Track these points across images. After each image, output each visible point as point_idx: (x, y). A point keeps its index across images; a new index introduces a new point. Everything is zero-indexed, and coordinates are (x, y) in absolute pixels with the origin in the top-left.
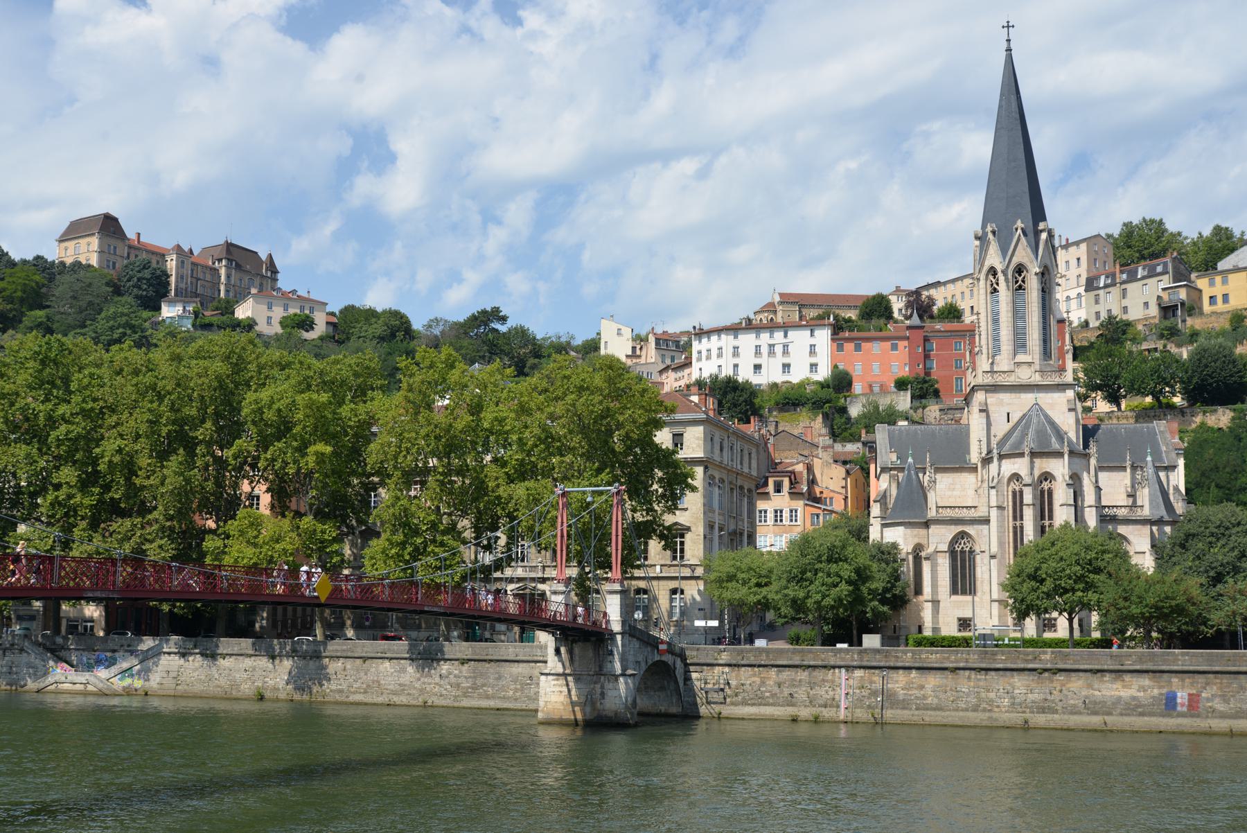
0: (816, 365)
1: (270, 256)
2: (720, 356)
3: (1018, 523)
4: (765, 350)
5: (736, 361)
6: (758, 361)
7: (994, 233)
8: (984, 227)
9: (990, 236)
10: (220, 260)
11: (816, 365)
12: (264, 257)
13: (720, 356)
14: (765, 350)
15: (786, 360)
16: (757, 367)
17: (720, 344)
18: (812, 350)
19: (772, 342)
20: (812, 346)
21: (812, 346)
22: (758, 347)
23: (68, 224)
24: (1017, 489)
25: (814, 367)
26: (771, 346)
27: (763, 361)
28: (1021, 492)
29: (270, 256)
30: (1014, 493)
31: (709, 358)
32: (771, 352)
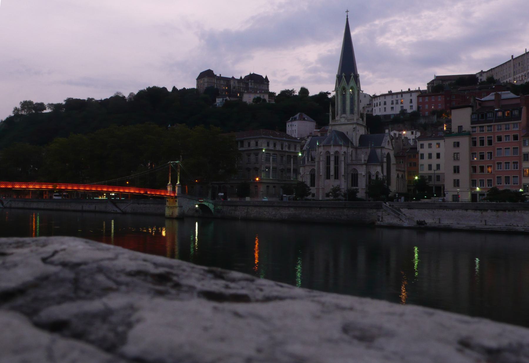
0: (412, 106)
1: (266, 77)
2: (380, 105)
3: (328, 166)
4: (395, 102)
5: (385, 106)
6: (392, 106)
7: (344, 76)
8: (341, 74)
9: (343, 77)
10: (248, 80)
11: (412, 106)
12: (264, 77)
13: (380, 105)
14: (395, 102)
15: (402, 105)
16: (392, 108)
17: (380, 101)
18: (411, 101)
19: (397, 99)
20: (411, 100)
21: (411, 100)
22: (392, 101)
23: (199, 74)
24: (328, 156)
25: (411, 106)
26: (397, 101)
27: (394, 106)
28: (330, 157)
29: (266, 77)
30: (327, 157)
31: (377, 106)
32: (397, 103)
